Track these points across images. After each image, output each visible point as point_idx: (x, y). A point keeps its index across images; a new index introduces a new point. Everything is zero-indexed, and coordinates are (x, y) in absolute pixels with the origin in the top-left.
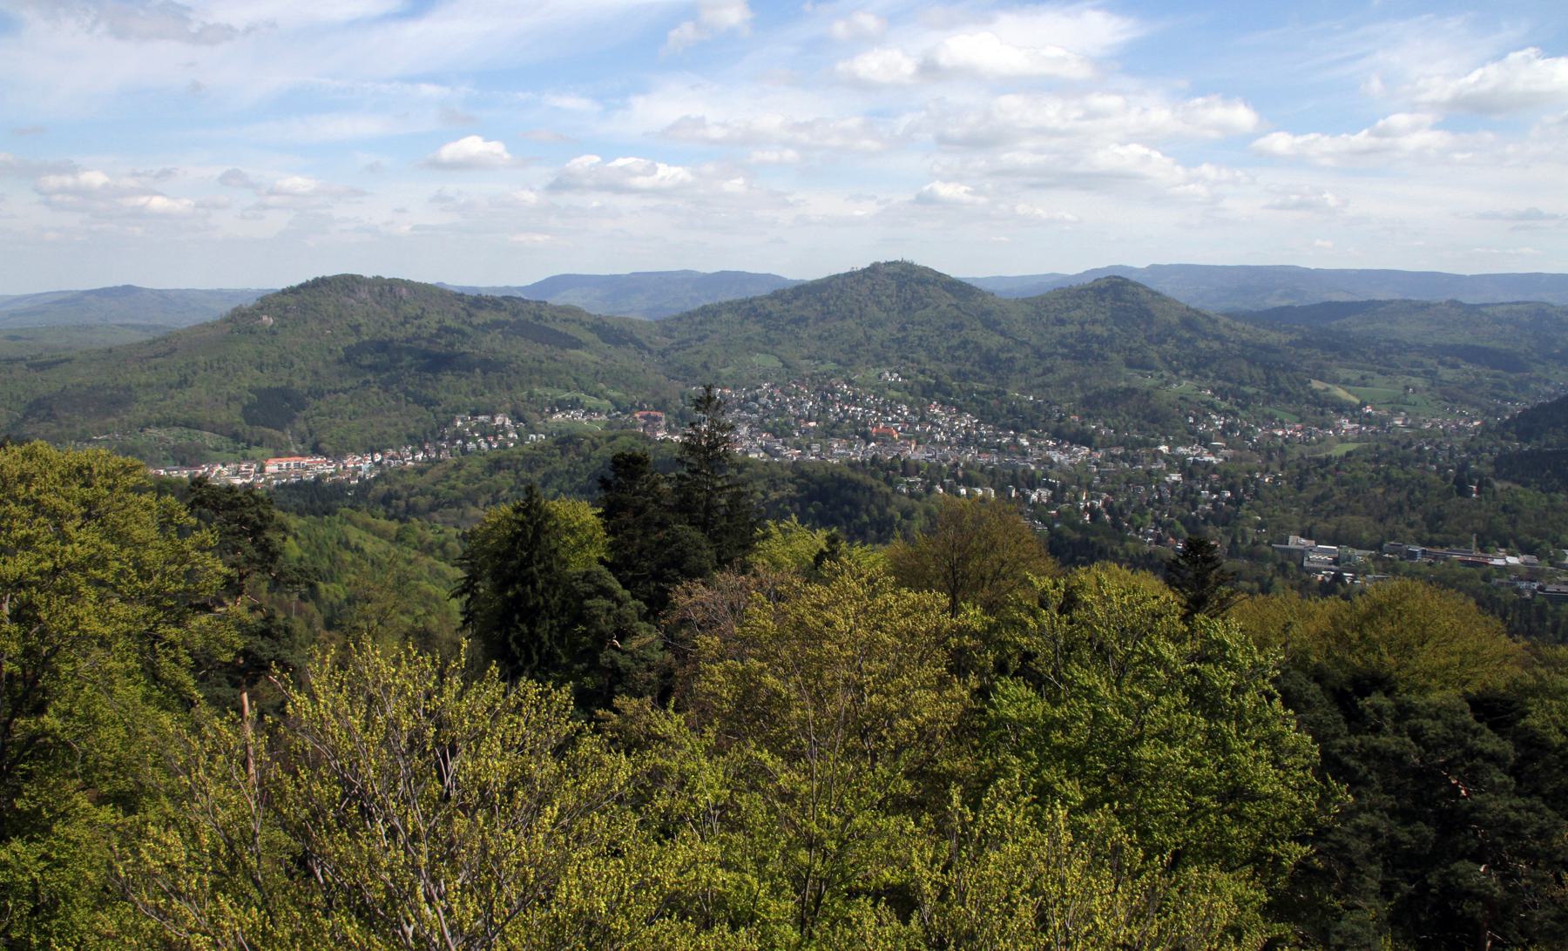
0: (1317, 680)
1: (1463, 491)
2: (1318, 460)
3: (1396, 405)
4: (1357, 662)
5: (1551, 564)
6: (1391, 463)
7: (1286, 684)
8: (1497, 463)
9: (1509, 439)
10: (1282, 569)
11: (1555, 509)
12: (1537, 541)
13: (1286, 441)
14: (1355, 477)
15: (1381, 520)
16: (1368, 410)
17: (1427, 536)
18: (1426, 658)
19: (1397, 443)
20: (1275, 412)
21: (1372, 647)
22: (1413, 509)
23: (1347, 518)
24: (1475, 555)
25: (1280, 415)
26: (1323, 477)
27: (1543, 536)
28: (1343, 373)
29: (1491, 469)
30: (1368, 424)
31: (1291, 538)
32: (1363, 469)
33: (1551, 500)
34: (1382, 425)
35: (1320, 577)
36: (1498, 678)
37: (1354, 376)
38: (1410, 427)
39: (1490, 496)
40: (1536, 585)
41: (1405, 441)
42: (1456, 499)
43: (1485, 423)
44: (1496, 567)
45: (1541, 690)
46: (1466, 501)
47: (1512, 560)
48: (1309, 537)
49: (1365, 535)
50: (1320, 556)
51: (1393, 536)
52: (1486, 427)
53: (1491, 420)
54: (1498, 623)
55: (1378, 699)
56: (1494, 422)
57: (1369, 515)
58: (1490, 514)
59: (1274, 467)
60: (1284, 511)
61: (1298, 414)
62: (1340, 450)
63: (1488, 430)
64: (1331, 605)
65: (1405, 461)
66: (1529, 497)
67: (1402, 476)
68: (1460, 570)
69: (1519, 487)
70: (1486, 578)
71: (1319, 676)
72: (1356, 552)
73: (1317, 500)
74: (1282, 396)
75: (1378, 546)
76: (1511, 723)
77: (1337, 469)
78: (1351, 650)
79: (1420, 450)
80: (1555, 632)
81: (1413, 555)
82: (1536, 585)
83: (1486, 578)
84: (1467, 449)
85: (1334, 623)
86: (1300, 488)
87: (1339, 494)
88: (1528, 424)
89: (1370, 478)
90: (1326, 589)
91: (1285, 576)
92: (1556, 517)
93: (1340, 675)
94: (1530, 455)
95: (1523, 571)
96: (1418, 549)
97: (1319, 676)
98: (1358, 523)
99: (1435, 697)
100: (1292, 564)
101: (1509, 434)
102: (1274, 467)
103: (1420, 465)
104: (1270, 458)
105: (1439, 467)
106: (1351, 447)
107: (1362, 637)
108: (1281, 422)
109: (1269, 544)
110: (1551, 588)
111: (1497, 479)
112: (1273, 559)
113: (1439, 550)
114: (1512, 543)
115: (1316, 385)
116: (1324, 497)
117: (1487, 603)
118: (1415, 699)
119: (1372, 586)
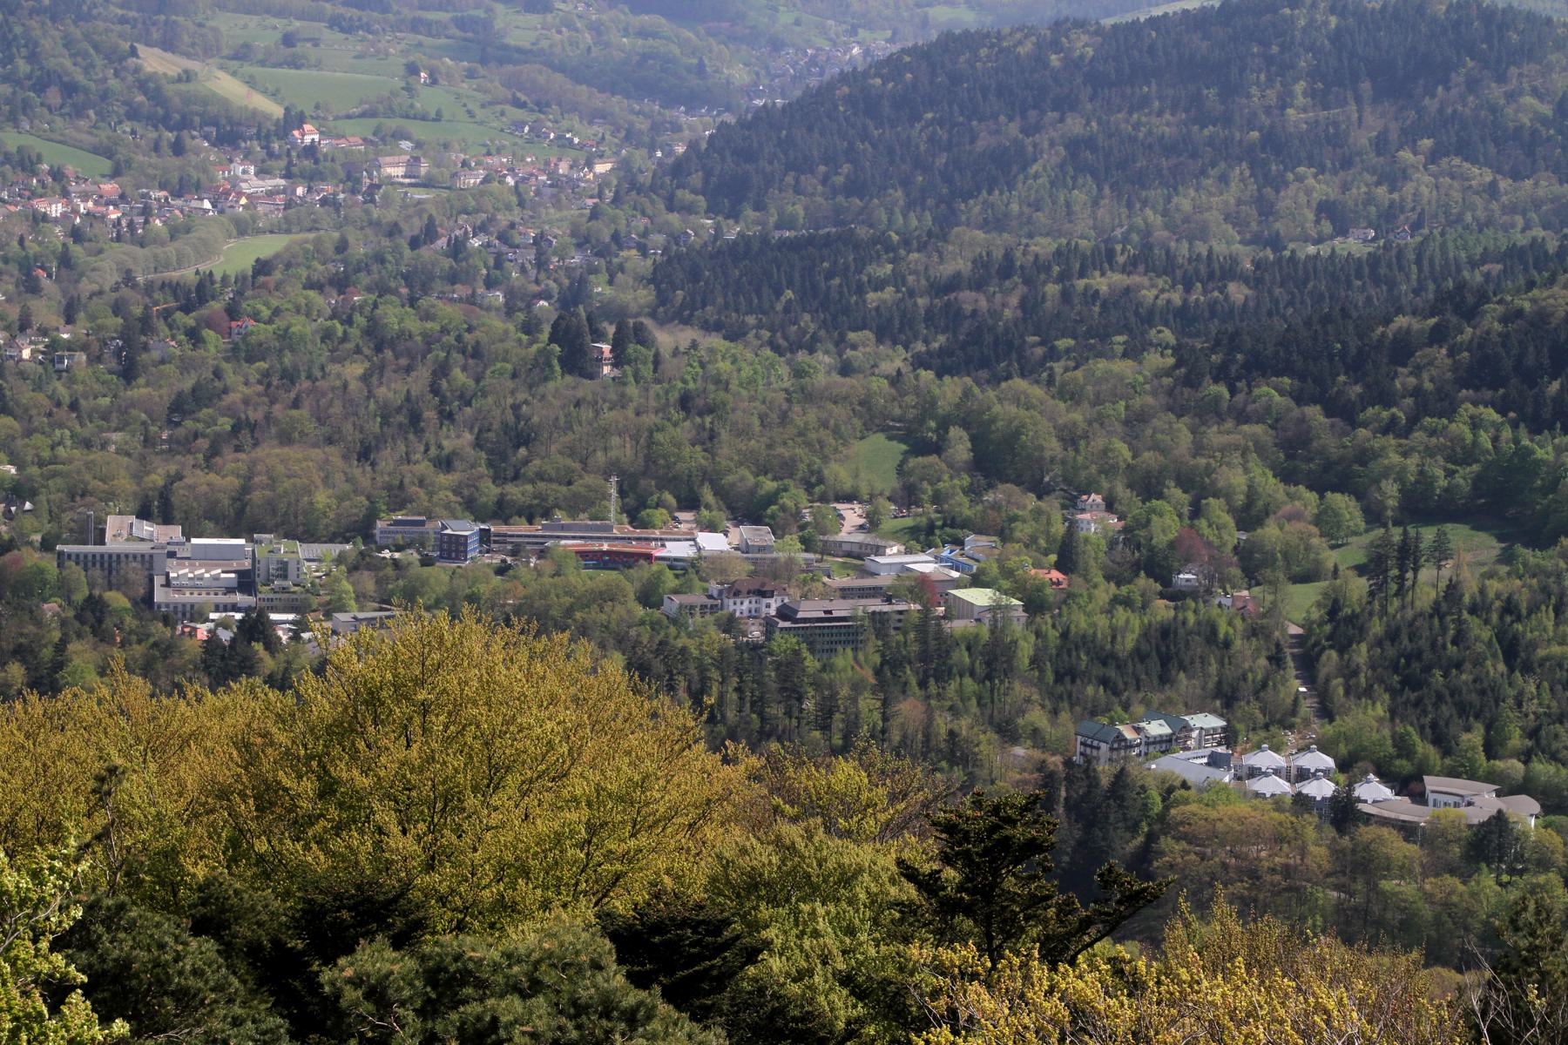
0: (200, 927)
1: (577, 362)
2: (174, 288)
3: (387, 119)
4: (317, 860)
5: (808, 545)
6: (382, 290)
7: (116, 947)
8: (659, 279)
9: (688, 209)
10: (92, 615)
11: (809, 396)
12: (769, 485)
13: (76, 235)
14: (284, 335)
15: (365, 454)
16: (310, 135)
17: (490, 491)
18: (507, 824)
19: (393, 231)
20: (36, 145)
21: (354, 812)
22: (447, 416)
23: (270, 453)
24: (618, 533)
25: (51, 155)
26: (194, 336)
27: (785, 469)
28: (231, 26)
29: (646, 295)
30: (311, 178)
31: (113, 524)
32: (308, 311)
33: (799, 373)
34: (351, 181)
35: (203, 630)
36: (675, 869)
37: (263, 32)
38: (427, 184)
39: (647, 371)
40: (774, 604)
41: (415, 226)
42: (561, 383)
43: (624, 166)
44: (673, 563)
45: (795, 885)
46: (586, 388)
47: (713, 542)
48: (167, 520)
49: (322, 498)
50: (199, 572)
51: (398, 498)
52: (628, 185)
53: (639, 158)
54: (680, 715)
55: (375, 958)
56: (646, 163)
57: (330, 441)
58: (650, 419)
59: (45, 311)
60: (87, 444)
61: (108, 153)
62: (234, 258)
63: (634, 186)
64: (242, 706)
65: (418, 283)
66: (746, 368)
67: (413, 325)
68: (584, 579)
69: (716, 341)
70: (649, 597)
71: (211, 918)
72: (303, 550)
73: (179, 408)
74: (54, 96)
75: (362, 529)
76: (723, 979)
77: (232, 312)
78: (299, 826)
79: (457, 249)
80: (825, 728)
81: (453, 548)
82: (774, 604)
83: (649, 597)
84: (583, 241)
85: (250, 758)
86: (128, 373)
87: (241, 384)
88: (732, 168)
89: (327, 335)
90: (224, 665)
91: (101, 636)
92: (812, 415)
93: (270, 905)
94: (739, 251)
95: (740, 571)
96: (467, 529)
97: (211, 918)
98: (310, 471)
99: (525, 936)
100: (117, 600)
101: (684, 195)
102: (45, 311)
103: (461, 291)
104: (33, 288)
105: (510, 295)
106: (269, 246)
107: (327, 790)
108: (57, 175)
109: (47, 545)
110: (810, 610)
111: (662, 323)
112: (64, 589)
113: (520, 528)
114: (708, 495)
115: (154, 61)
116: (200, 397)
117: (654, 667)
118: (479, 948)
119: (351, 640)
